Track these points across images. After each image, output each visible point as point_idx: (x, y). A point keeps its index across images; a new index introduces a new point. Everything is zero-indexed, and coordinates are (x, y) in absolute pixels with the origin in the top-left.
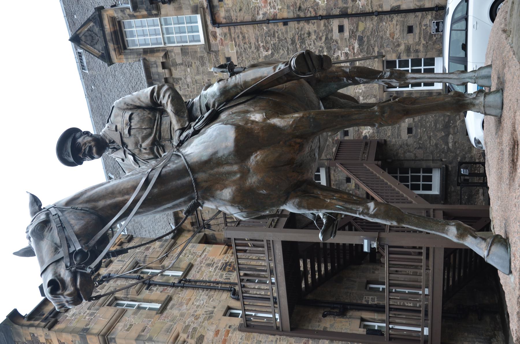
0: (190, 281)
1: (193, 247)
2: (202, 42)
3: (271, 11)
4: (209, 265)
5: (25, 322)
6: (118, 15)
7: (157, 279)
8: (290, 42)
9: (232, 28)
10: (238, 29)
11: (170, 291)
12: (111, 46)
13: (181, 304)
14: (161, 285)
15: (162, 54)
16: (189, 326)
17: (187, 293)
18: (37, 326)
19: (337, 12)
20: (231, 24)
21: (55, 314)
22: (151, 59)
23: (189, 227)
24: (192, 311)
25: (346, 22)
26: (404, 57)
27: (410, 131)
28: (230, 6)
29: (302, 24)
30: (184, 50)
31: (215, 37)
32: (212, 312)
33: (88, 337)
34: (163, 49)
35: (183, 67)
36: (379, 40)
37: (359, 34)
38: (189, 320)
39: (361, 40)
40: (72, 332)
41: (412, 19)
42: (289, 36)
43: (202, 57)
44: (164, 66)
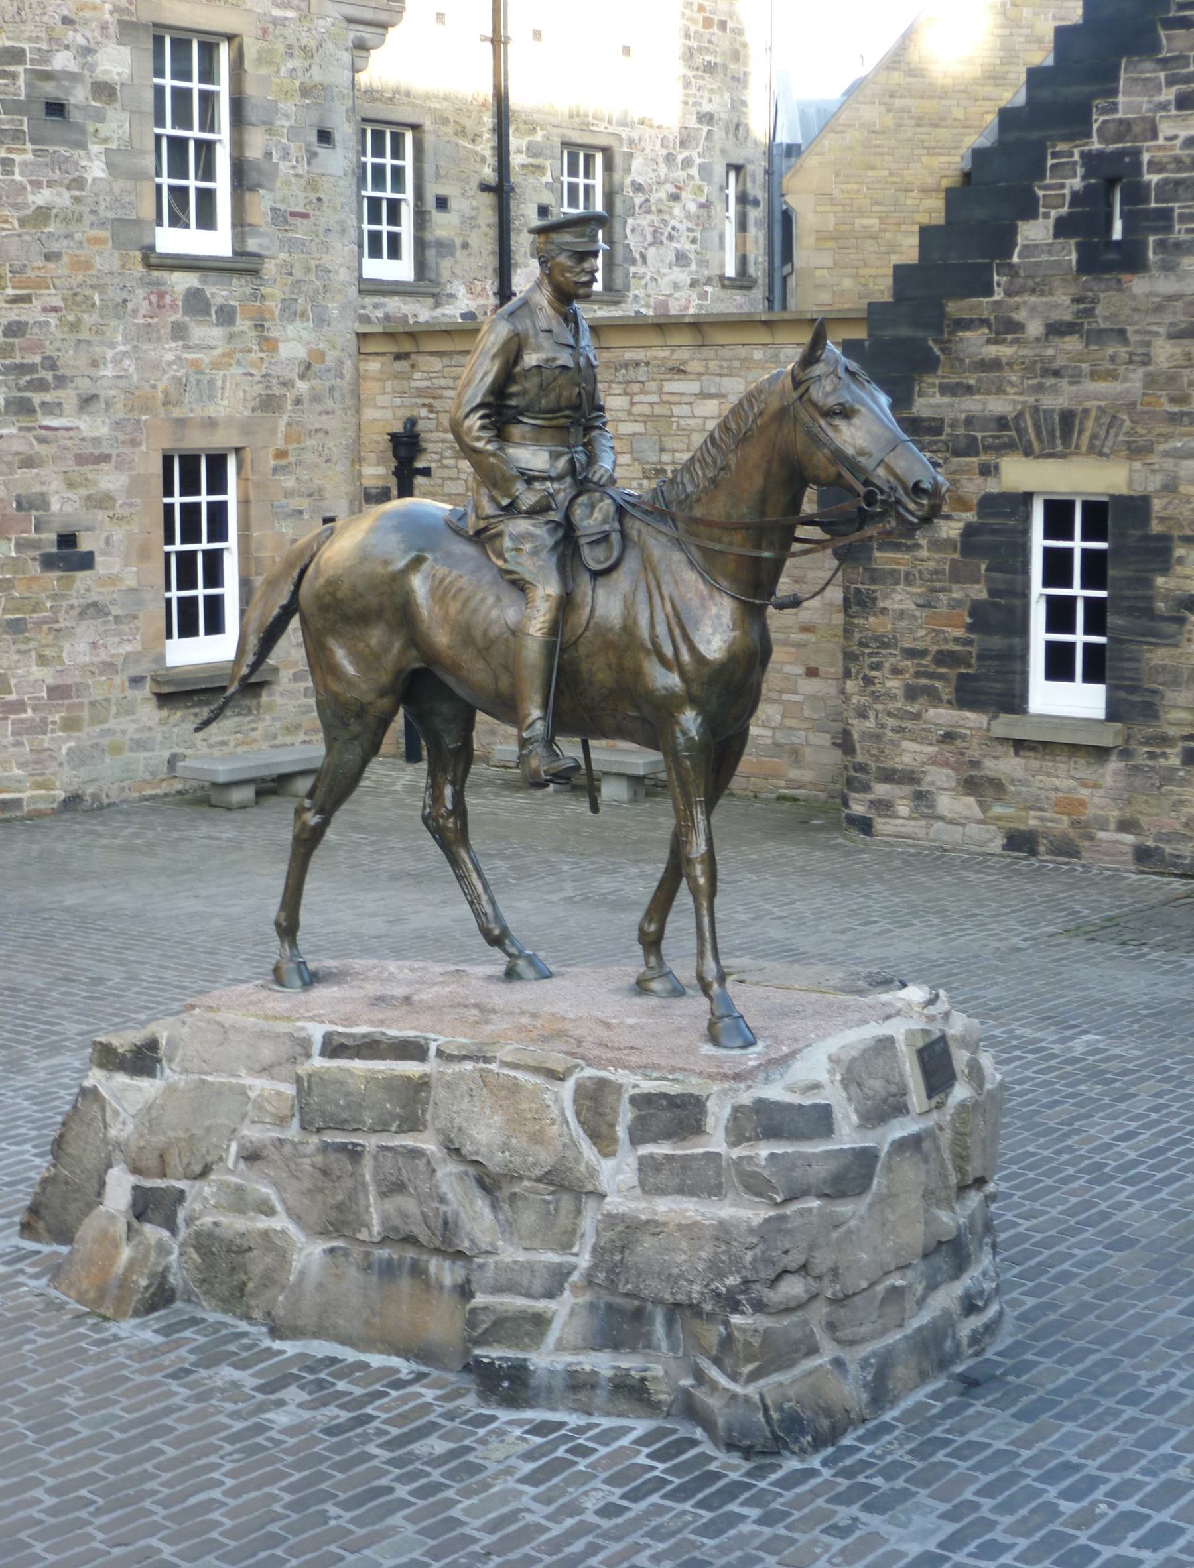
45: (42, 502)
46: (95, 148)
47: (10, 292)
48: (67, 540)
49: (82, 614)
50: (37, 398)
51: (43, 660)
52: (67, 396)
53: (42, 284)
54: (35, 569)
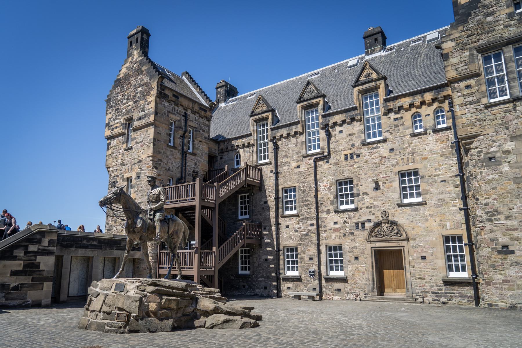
0: (186, 157)
1: (206, 153)
3: (320, 189)
6: (320, 107)
7: (186, 140)
8: (307, 199)
9: (313, 169)
10: (313, 172)
11: (180, 148)
12: (305, 103)
13: (173, 155)
14: (183, 142)
15: (301, 131)
16: (161, 161)
17: (179, 156)
18: (157, 90)
23: (221, 148)
24: (170, 161)
25: (315, 227)
26: (299, 256)
28: (324, 167)
29: (315, 205)
31: (309, 160)
32: (169, 171)
33: (153, 115)
35: (295, 142)
36: (306, 244)
37: (309, 233)
39: (307, 235)
41: (316, 259)
42: (309, 198)
43: (300, 153)
44: (296, 133)
45: (497, 240)
46: (505, 164)
47: (484, 197)
49: (512, 264)
50: (493, 218)
51: (501, 274)
52: (502, 217)
53: (492, 194)
54: (496, 253)
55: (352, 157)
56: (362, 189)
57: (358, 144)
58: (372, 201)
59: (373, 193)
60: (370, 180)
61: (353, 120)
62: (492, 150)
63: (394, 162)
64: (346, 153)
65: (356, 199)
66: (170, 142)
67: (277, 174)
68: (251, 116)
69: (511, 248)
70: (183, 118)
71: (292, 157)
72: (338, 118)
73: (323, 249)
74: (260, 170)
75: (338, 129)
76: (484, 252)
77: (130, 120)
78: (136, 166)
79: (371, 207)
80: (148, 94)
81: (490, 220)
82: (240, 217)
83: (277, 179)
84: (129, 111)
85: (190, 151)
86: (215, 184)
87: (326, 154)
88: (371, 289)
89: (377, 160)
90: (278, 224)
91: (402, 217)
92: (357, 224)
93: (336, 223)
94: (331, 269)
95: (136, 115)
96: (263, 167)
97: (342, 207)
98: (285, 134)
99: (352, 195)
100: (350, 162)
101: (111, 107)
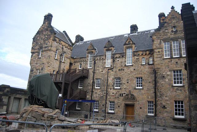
2: (106, 67)
4: (64, 66)
5: (54, 35)
6: (112, 50)
7: (62, 57)
16: (51, 64)
18: (53, 38)
19: (107, 93)
20: (108, 72)
21: (55, 40)
22: (104, 56)
25: (106, 94)
27: (87, 104)
30: (105, 63)
31: (107, 69)
34: (106, 59)
38: (53, 64)
39: (102, 97)
40: (52, 44)
41: (105, 106)
46: (167, 79)
48: (164, 106)
52: (164, 96)
55: (121, 70)
56: (123, 82)
57: (123, 66)
58: (126, 87)
59: (127, 84)
60: (126, 79)
61: (123, 56)
62: (163, 74)
63: (135, 74)
64: (119, 68)
65: (121, 85)
66: (55, 57)
67: (94, 73)
68: (87, 50)
69: (166, 107)
70: (62, 49)
71: (100, 68)
72: (117, 56)
73: (108, 102)
74: (88, 71)
75: (118, 59)
76: (159, 107)
77: (41, 48)
78: (42, 65)
79: (126, 89)
80: (50, 39)
81: (161, 97)
82: (79, 88)
83: (94, 75)
84: (41, 44)
85: (63, 61)
86: (71, 75)
87: (112, 68)
88: (122, 117)
89: (129, 72)
90: (92, 92)
91: (135, 94)
92: (120, 95)
93: (113, 93)
94: (110, 110)
95: (44, 46)
96: (89, 70)
97: (115, 88)
98: (99, 59)
99: (120, 84)
100: (120, 72)
101: (34, 41)
